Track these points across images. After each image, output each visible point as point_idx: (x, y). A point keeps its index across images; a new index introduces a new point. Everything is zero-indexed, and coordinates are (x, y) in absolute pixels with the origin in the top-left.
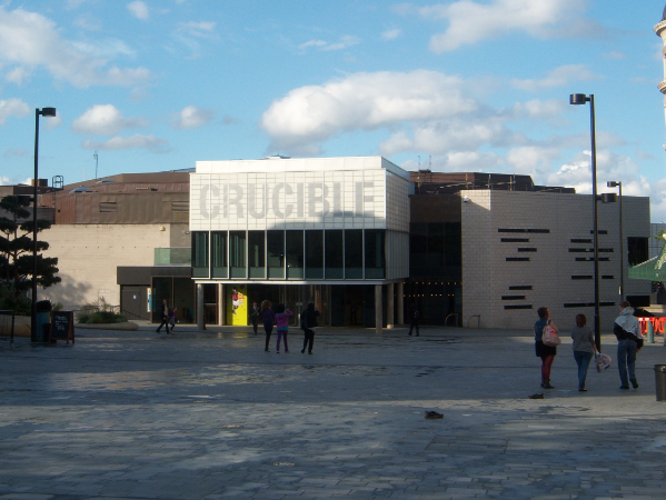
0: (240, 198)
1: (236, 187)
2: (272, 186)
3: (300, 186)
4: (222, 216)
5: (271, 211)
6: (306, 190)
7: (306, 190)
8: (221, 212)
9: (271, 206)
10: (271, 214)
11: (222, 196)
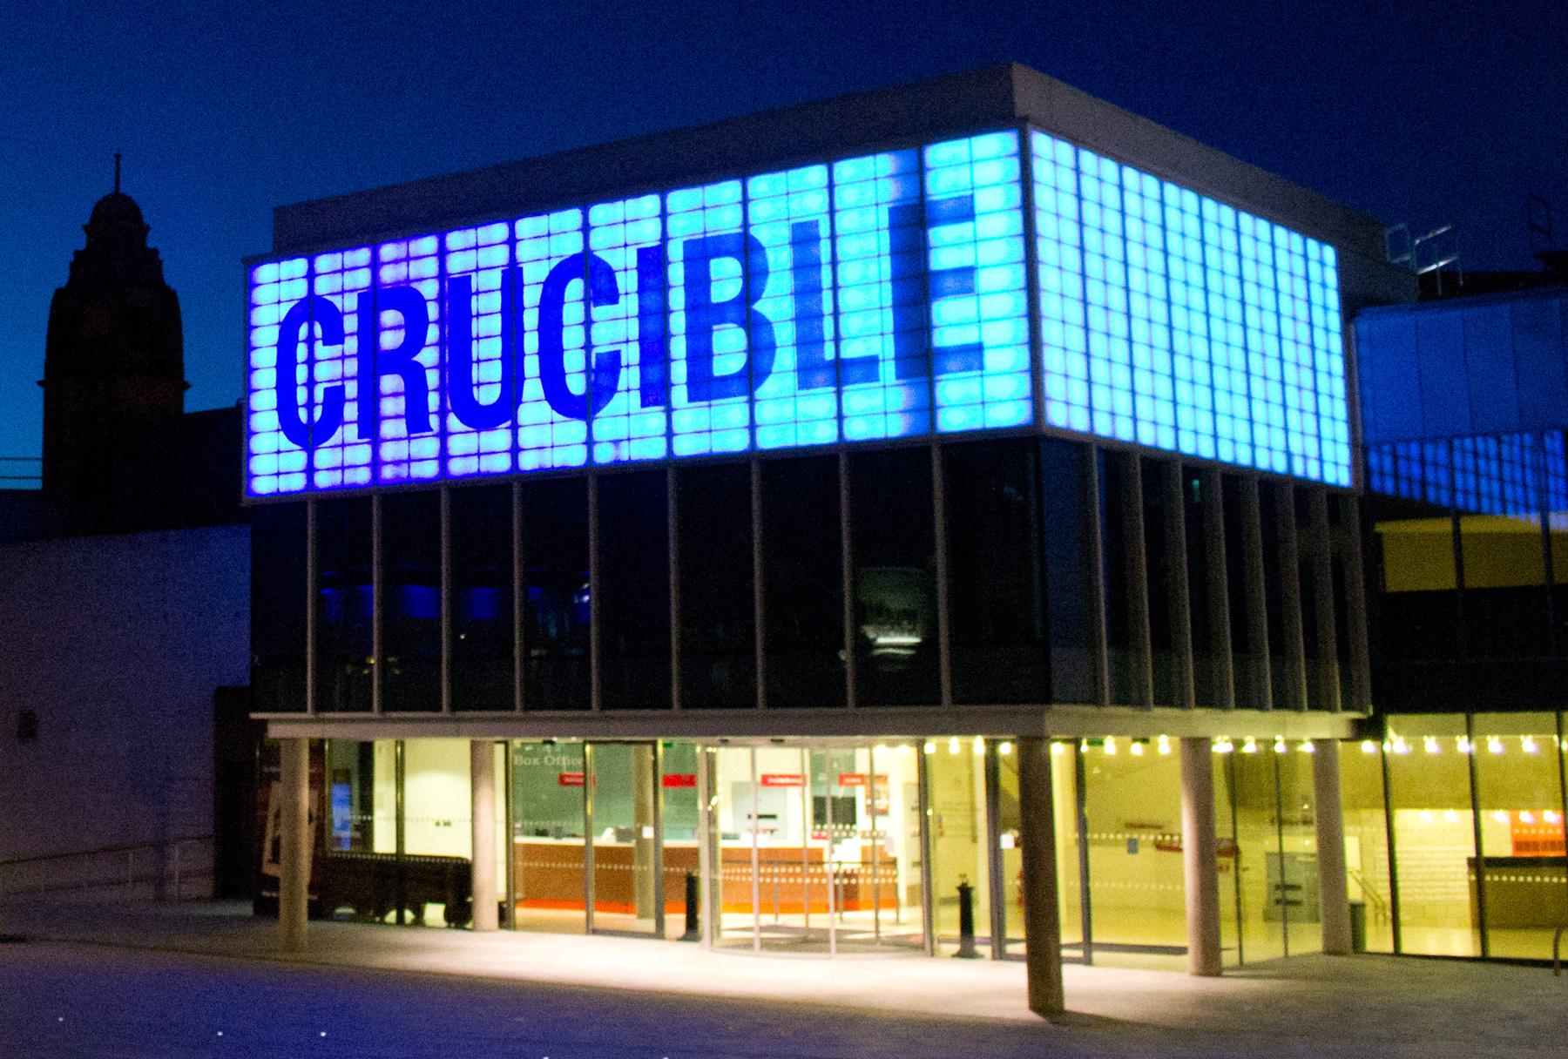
0: (415, 341)
1: (405, 297)
2: (535, 275)
3: (652, 262)
4: (351, 432)
5: (533, 388)
6: (676, 273)
7: (676, 273)
8: (351, 411)
9: (532, 365)
10: (534, 407)
11: (351, 345)
